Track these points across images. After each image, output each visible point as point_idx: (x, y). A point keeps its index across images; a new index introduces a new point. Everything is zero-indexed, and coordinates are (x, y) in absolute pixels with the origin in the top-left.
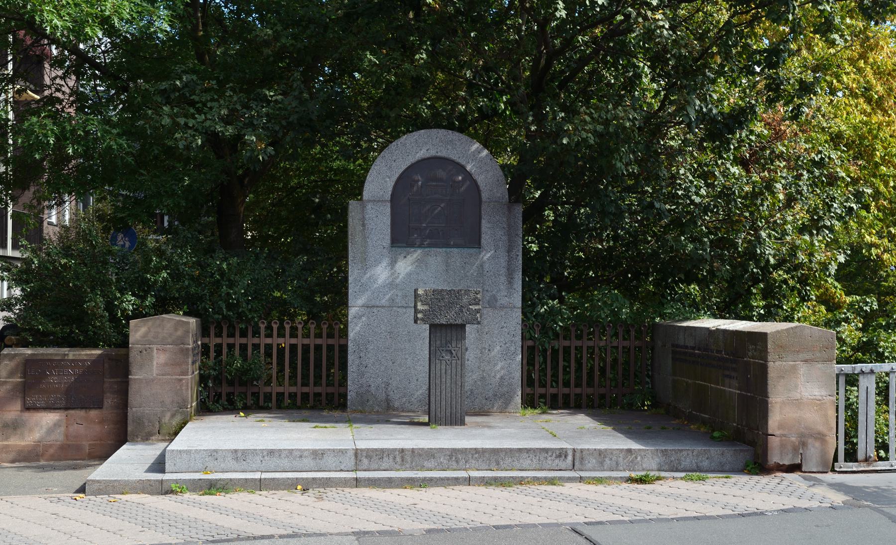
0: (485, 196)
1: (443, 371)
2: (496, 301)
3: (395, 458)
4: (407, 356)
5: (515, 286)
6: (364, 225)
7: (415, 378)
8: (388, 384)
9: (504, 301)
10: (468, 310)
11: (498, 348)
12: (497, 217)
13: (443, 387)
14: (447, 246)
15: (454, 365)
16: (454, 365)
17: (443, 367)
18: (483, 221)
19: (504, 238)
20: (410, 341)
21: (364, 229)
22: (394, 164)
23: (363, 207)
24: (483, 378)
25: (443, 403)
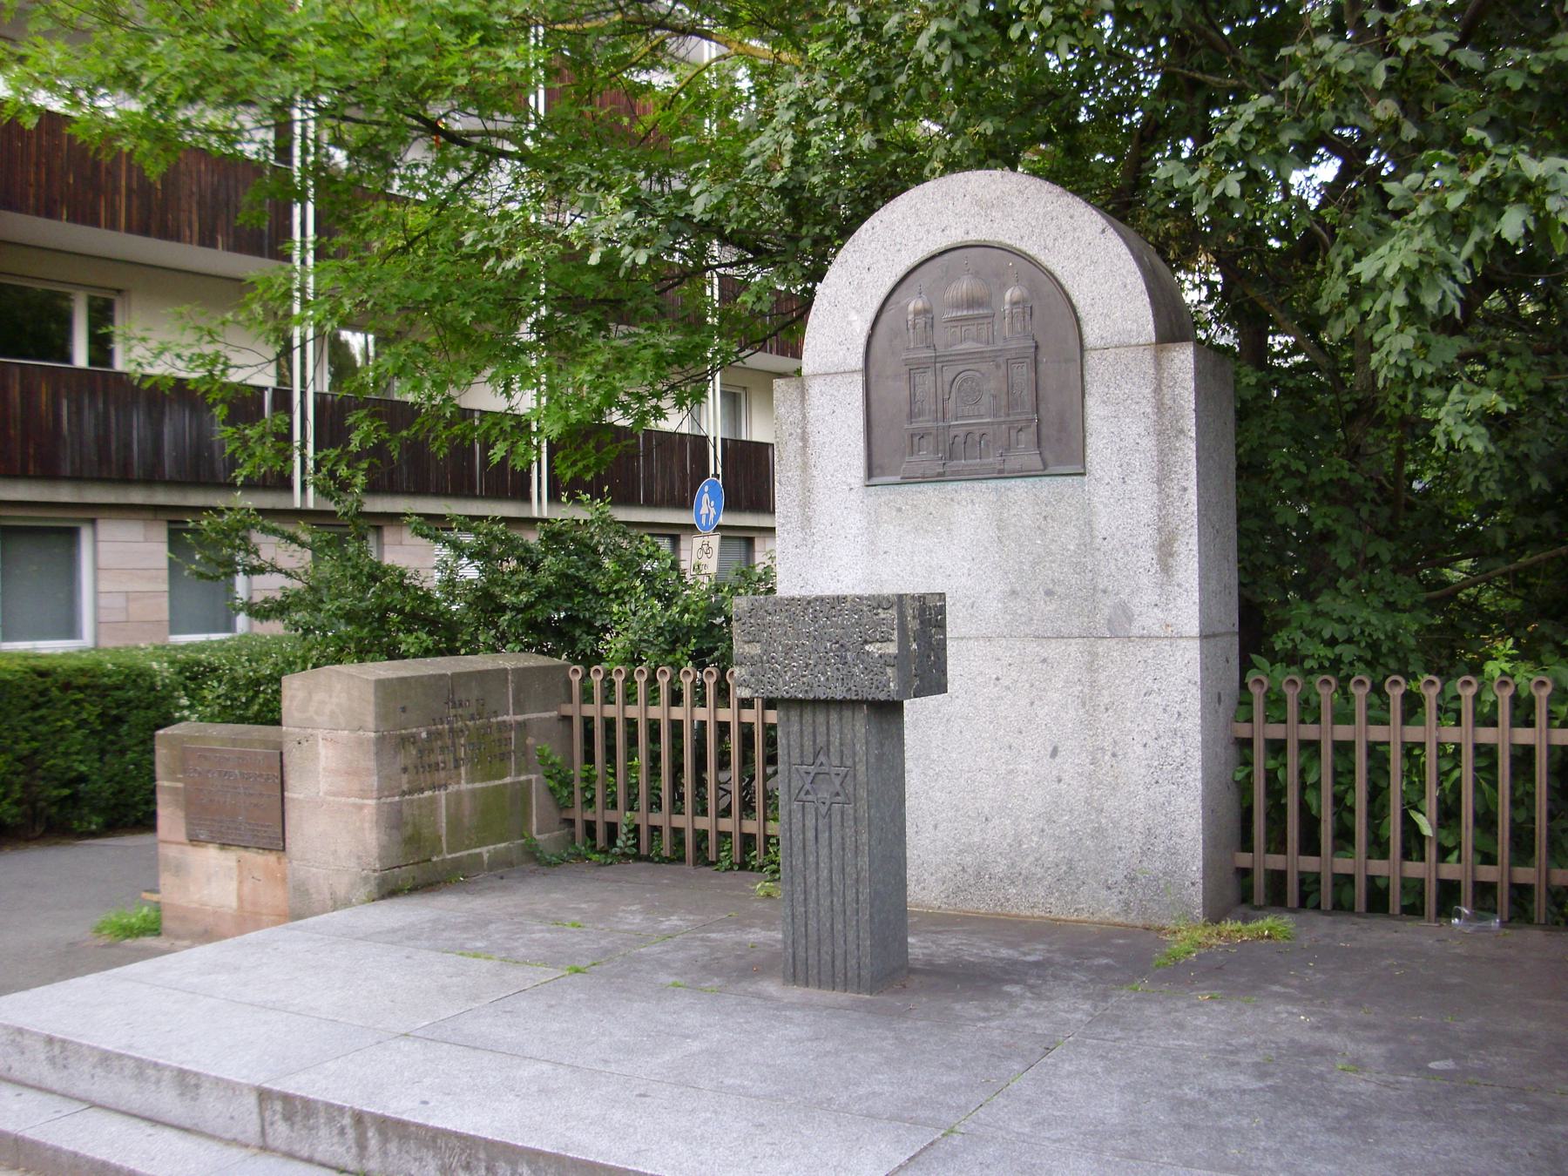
0: (1092, 334)
1: (810, 835)
2: (1130, 620)
3: (342, 1132)
5: (1180, 576)
6: (804, 438)
9: (1148, 620)
10: (861, 654)
11: (1139, 749)
12: (1127, 388)
13: (812, 879)
14: (1002, 475)
15: (837, 819)
16: (837, 819)
17: (810, 823)
18: (1091, 402)
19: (1149, 443)
21: (805, 447)
22: (868, 277)
24: (1099, 832)
25: (812, 923)
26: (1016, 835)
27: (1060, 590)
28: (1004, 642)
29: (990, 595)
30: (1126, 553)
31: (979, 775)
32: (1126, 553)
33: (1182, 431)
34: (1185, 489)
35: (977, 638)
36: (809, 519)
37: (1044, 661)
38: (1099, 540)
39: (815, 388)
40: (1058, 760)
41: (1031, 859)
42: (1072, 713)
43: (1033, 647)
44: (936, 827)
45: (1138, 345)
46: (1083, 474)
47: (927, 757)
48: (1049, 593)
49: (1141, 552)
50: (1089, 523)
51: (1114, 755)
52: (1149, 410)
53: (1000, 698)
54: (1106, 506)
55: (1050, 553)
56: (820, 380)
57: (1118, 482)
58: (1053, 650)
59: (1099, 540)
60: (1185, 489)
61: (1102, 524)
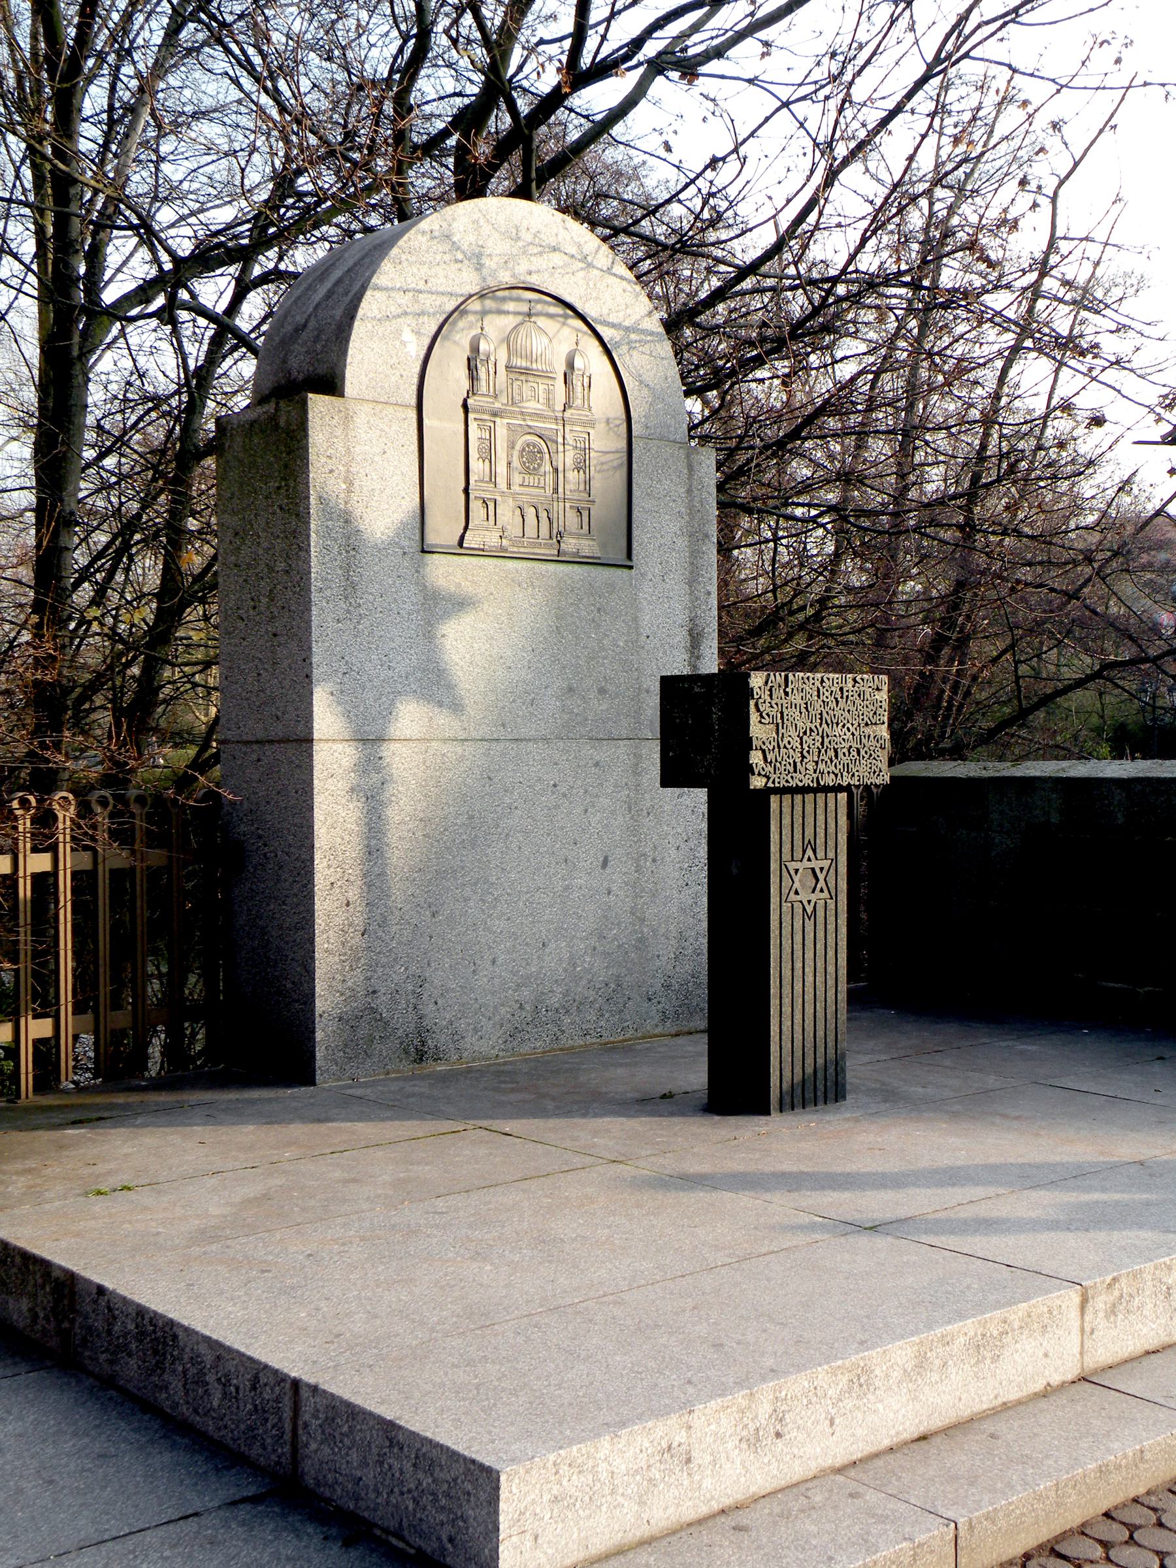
4: (468, 892)
7: (488, 956)
8: (422, 982)
11: (673, 852)
19: (682, 543)
20: (473, 843)
23: (347, 419)
26: (571, 957)
27: (611, 688)
28: (561, 744)
29: (549, 692)
30: (665, 653)
31: (537, 896)
32: (665, 653)
33: (707, 536)
34: (709, 593)
35: (535, 740)
36: (353, 586)
37: (597, 764)
38: (643, 638)
39: (363, 415)
40: (608, 870)
41: (584, 982)
42: (620, 818)
43: (588, 750)
44: (494, 962)
45: (674, 441)
46: (631, 567)
47: (486, 881)
48: (602, 691)
49: (676, 652)
50: (635, 619)
51: (654, 860)
52: (683, 510)
53: (557, 807)
54: (649, 603)
55: (603, 649)
56: (367, 408)
57: (658, 579)
58: (603, 753)
59: (643, 638)
60: (709, 593)
61: (646, 619)
